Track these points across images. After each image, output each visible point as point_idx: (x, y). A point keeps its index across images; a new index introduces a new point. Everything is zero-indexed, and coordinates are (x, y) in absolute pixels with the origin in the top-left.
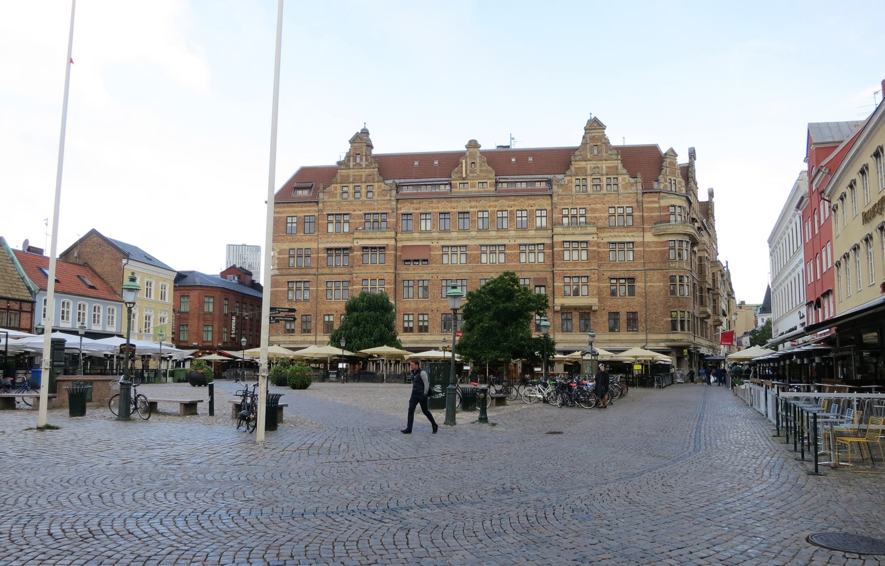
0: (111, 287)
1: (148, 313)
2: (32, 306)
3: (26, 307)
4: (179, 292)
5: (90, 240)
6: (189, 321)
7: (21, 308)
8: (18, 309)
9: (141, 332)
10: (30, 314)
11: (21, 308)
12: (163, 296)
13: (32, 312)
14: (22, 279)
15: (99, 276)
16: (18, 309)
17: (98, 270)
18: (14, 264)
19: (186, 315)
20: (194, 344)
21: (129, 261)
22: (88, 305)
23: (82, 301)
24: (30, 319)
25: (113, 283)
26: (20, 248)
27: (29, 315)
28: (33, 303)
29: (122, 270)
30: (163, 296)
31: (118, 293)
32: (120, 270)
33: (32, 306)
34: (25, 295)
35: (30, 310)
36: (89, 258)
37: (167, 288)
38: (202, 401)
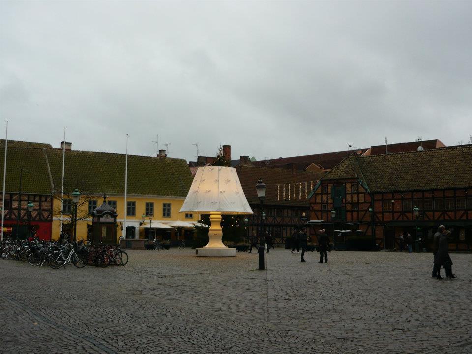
38: (262, 267)
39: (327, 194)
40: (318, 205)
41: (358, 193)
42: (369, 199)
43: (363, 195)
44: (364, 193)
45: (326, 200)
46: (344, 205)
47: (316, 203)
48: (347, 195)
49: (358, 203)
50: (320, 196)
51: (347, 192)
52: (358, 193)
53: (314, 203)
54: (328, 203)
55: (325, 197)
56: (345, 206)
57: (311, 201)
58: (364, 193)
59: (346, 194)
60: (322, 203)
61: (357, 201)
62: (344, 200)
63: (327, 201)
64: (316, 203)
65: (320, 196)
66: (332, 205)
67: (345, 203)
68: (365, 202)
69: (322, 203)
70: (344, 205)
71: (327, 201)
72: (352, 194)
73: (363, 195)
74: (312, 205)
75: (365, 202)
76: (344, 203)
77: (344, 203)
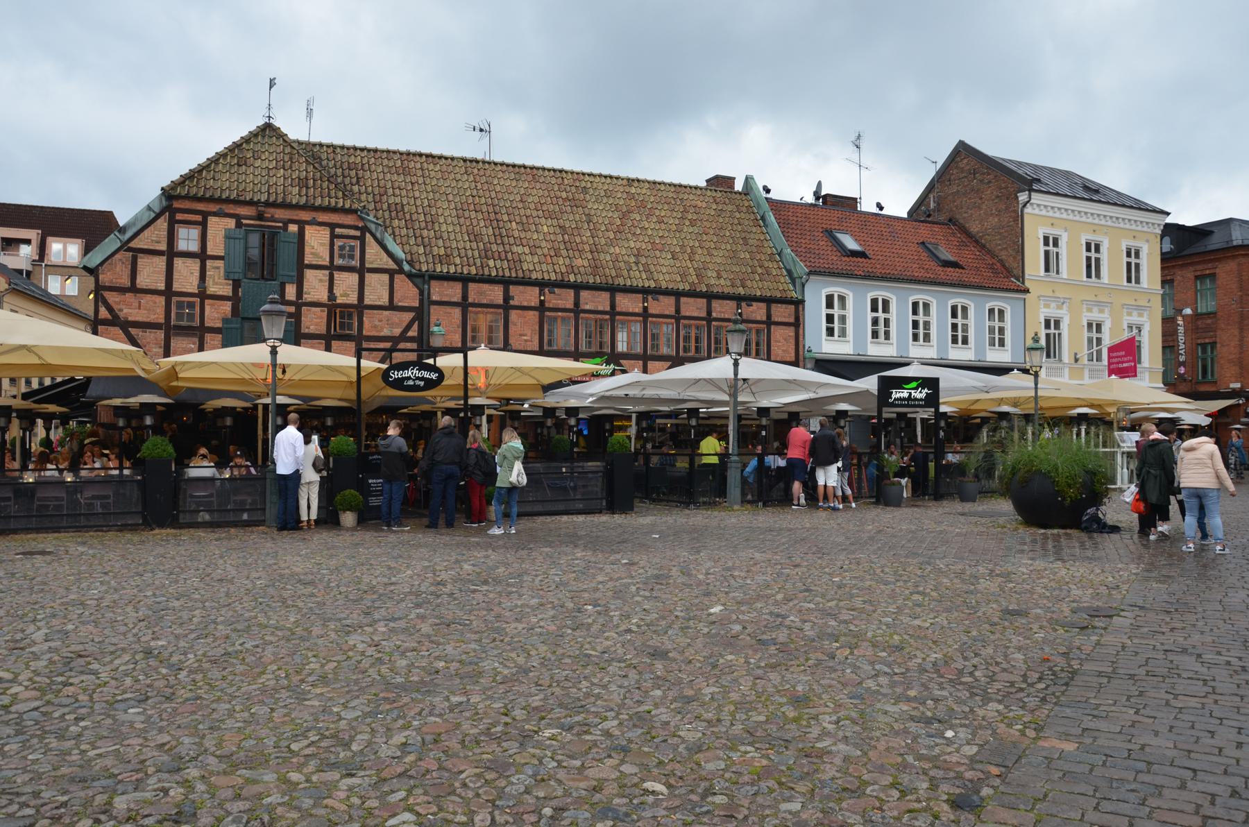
0: (1001, 261)
1: (1095, 316)
2: (797, 311)
3: (782, 313)
4: (1192, 269)
5: (957, 168)
6: (1219, 333)
7: (769, 316)
8: (764, 318)
9: (1076, 360)
10: (792, 328)
11: (769, 316)
12: (1132, 273)
13: (797, 323)
14: (779, 255)
15: (977, 242)
16: (764, 318)
17: (974, 228)
18: (766, 226)
19: (1209, 321)
20: (1233, 385)
21: (1034, 195)
22: (939, 303)
23: (920, 295)
24: (793, 341)
25: (1003, 253)
26: (810, 199)
27: (790, 332)
28: (799, 303)
29: (1019, 219)
30: (1132, 273)
31: (1015, 272)
32: (1016, 220)
33: (797, 311)
34: (783, 287)
35: (792, 320)
36: (956, 207)
37: (1143, 254)
40: (147, 300)
41: (362, 271)
43: (385, 278)
44: (391, 273)
46: (292, 309)
48: (309, 274)
49: (361, 307)
50: (161, 262)
52: (362, 271)
53: (121, 290)
54: (203, 295)
58: (391, 273)
60: (168, 292)
61: (353, 299)
64: (133, 289)
66: (227, 307)
68: (392, 307)
72: (332, 268)
73: (386, 277)
74: (112, 298)
76: (289, 303)
77: (289, 303)
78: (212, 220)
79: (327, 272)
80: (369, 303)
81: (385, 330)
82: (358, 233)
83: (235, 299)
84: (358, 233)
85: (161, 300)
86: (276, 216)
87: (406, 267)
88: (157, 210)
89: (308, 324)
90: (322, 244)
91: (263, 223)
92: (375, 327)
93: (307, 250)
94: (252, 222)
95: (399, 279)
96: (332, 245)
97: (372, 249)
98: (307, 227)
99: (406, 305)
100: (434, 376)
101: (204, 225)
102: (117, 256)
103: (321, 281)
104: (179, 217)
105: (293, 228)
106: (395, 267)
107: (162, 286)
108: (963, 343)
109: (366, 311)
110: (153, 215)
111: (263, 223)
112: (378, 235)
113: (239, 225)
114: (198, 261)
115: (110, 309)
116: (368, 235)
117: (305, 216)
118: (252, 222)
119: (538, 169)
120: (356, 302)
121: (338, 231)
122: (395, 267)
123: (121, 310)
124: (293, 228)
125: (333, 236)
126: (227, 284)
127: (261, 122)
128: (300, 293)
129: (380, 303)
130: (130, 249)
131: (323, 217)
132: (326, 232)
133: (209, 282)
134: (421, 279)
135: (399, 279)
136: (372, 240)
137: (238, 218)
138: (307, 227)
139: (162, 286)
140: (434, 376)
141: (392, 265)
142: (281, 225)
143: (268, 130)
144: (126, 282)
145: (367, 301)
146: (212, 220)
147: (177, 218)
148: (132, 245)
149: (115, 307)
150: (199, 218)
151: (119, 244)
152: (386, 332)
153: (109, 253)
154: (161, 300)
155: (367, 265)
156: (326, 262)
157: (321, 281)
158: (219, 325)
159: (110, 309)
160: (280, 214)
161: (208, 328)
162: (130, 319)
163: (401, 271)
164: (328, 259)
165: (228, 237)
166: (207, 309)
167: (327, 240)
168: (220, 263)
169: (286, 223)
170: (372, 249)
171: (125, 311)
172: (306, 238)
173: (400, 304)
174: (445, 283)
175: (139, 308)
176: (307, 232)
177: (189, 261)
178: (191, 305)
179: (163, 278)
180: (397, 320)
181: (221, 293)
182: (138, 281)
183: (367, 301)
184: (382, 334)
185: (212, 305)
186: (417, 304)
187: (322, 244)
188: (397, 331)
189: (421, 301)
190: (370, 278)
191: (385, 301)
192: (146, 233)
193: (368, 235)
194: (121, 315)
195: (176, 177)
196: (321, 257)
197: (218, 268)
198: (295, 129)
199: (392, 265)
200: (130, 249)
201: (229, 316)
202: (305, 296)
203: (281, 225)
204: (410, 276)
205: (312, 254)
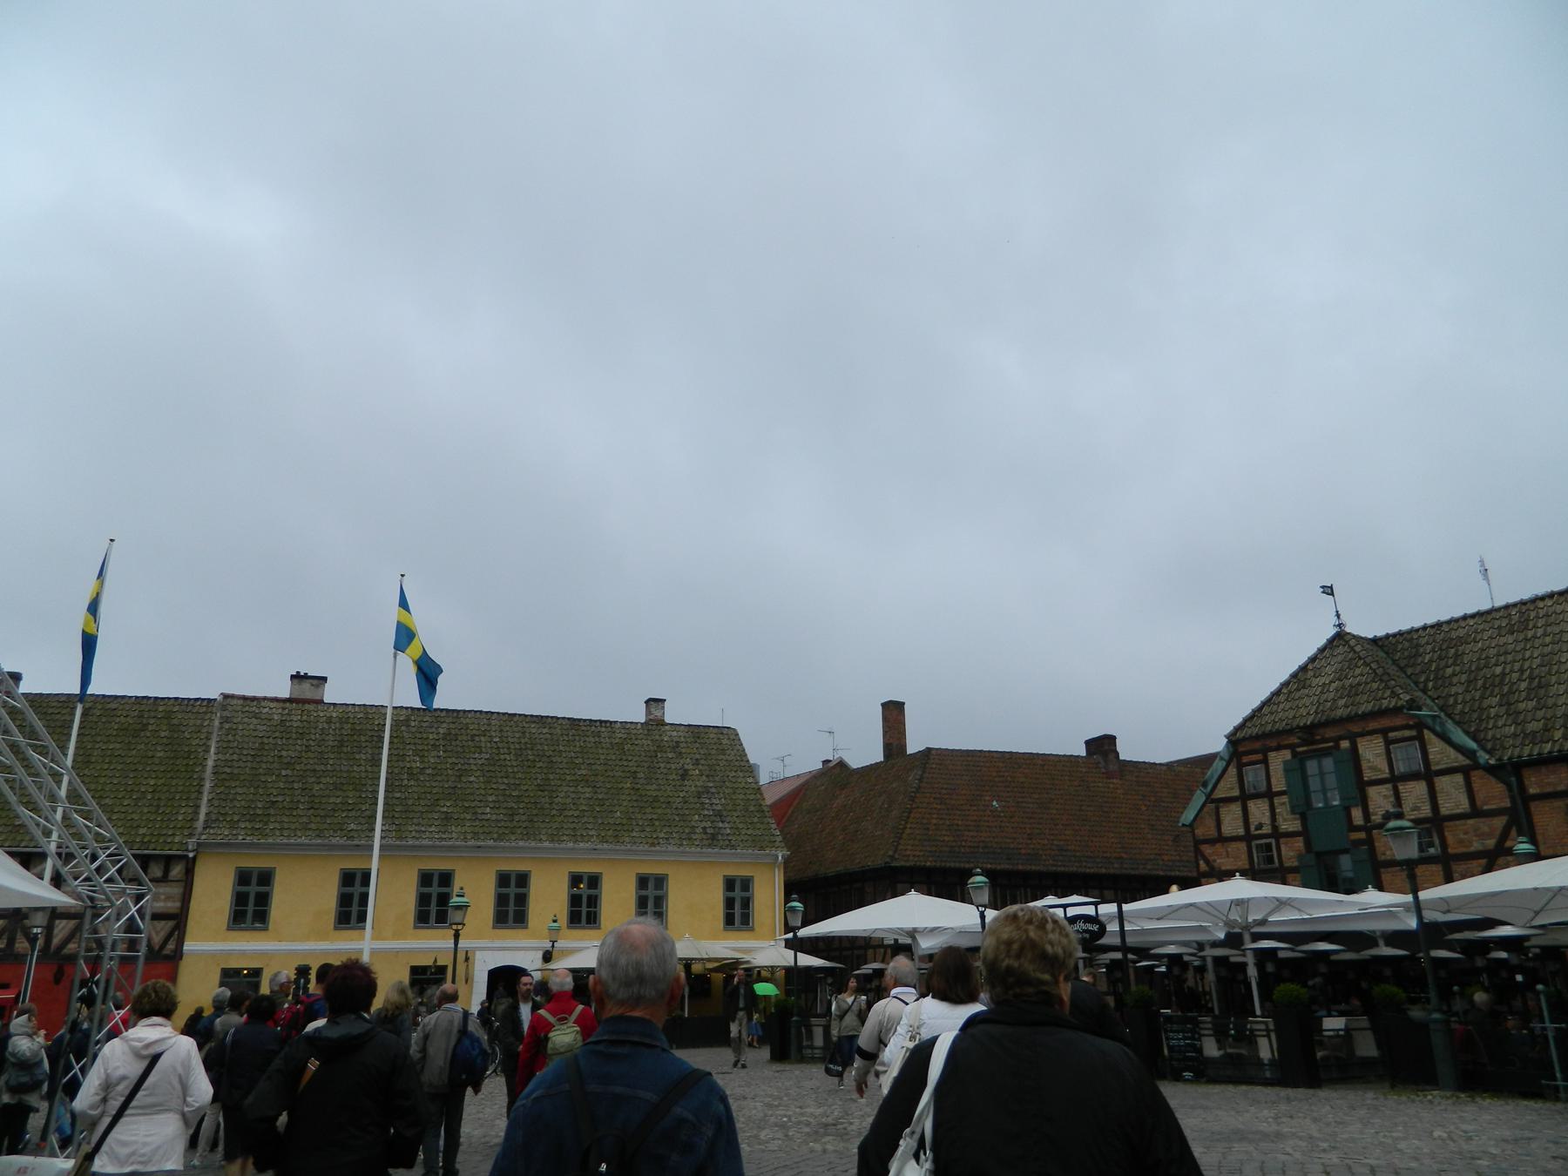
39: (1270, 795)
40: (1234, 846)
42: (1494, 793)
43: (1459, 778)
44: (1465, 771)
45: (1266, 820)
46: (1362, 835)
47: (1222, 839)
48: (1372, 792)
50: (1236, 809)
51: (1368, 775)
52: (1428, 775)
53: (1212, 842)
54: (1276, 834)
55: (1259, 810)
56: (1370, 842)
57: (1199, 832)
58: (1465, 771)
59: (1362, 785)
62: (1357, 815)
63: (1275, 827)
64: (1222, 839)
65: (1236, 809)
66: (1299, 843)
67: (1368, 827)
68: (1476, 812)
69: (1248, 838)
70: (1362, 835)
71: (1275, 827)
72: (1395, 780)
73: (1459, 778)
75: (1476, 812)
78: (1272, 755)
79: (1389, 786)
80: (1447, 813)
81: (1475, 844)
82: (1413, 733)
83: (1304, 833)
84: (1413, 733)
85: (1243, 846)
86: (1327, 736)
87: (1483, 757)
88: (1227, 758)
89: (1383, 849)
90: (1378, 755)
91: (1315, 747)
92: (1461, 842)
93: (1364, 765)
94: (1305, 748)
95: (1476, 776)
96: (1388, 753)
97: (1436, 748)
98: (1359, 740)
99: (1494, 807)
100: (1096, 928)
101: (1265, 762)
102: (1205, 810)
103: (1385, 797)
104: (1245, 759)
105: (1345, 744)
106: (1468, 762)
107: (1241, 832)
108: (588, 922)
109: (1446, 824)
110: (1225, 763)
111: (1315, 747)
112: (1438, 728)
113: (1295, 754)
114: (1266, 800)
115: (1207, 862)
116: (1426, 731)
117: (1356, 728)
118: (1305, 748)
119: (1542, 598)
120: (1430, 815)
121: (1392, 735)
122: (1468, 762)
123: (1215, 861)
124: (1345, 744)
125: (1388, 743)
126: (1295, 819)
127: (1332, 631)
128: (1367, 814)
129: (1458, 811)
130: (1213, 801)
131: (1373, 725)
132: (1378, 742)
133: (1280, 819)
134: (1511, 772)
135: (1476, 776)
136: (1433, 736)
137: (1292, 747)
138: (1359, 740)
139: (1241, 832)
140: (1096, 928)
141: (1462, 760)
142: (1331, 744)
143: (1340, 637)
144: (1213, 833)
145: (1444, 811)
146: (1272, 755)
147: (1244, 761)
148: (1212, 797)
149: (1211, 858)
150: (1259, 757)
151: (1204, 798)
152: (1476, 846)
153: (1199, 807)
154: (1243, 846)
155: (1434, 768)
156: (1386, 775)
157: (1385, 797)
158: (1296, 864)
159: (1207, 862)
160: (1330, 733)
161: (1288, 868)
162: (1223, 868)
163: (1476, 766)
164: (1387, 771)
165: (1287, 770)
166: (1283, 847)
167: (1381, 749)
168: (1285, 799)
169: (1337, 740)
170: (1436, 748)
171: (1218, 861)
172: (1360, 752)
173: (1485, 807)
174: (1544, 769)
175: (1228, 857)
176: (1359, 746)
177: (1259, 801)
178: (1269, 846)
179: (1240, 823)
180: (1486, 829)
181: (1291, 830)
182: (1223, 830)
183: (1444, 811)
184: (1472, 849)
185: (1286, 844)
186: (1507, 803)
187: (1378, 755)
188: (1491, 843)
189: (1513, 799)
190: (1443, 783)
191: (1464, 805)
192: (1222, 784)
193: (1426, 731)
194: (1216, 865)
195: (1238, 721)
196: (1380, 770)
197: (1284, 803)
198: (1368, 625)
199: (1462, 760)
200: (1213, 801)
201: (1304, 851)
202: (1373, 818)
203: (1331, 744)
204: (1490, 770)
205: (1370, 768)
